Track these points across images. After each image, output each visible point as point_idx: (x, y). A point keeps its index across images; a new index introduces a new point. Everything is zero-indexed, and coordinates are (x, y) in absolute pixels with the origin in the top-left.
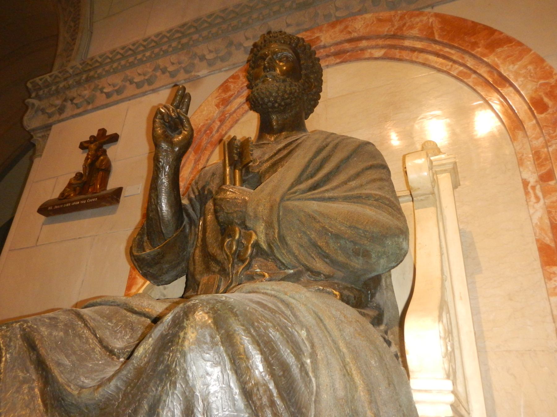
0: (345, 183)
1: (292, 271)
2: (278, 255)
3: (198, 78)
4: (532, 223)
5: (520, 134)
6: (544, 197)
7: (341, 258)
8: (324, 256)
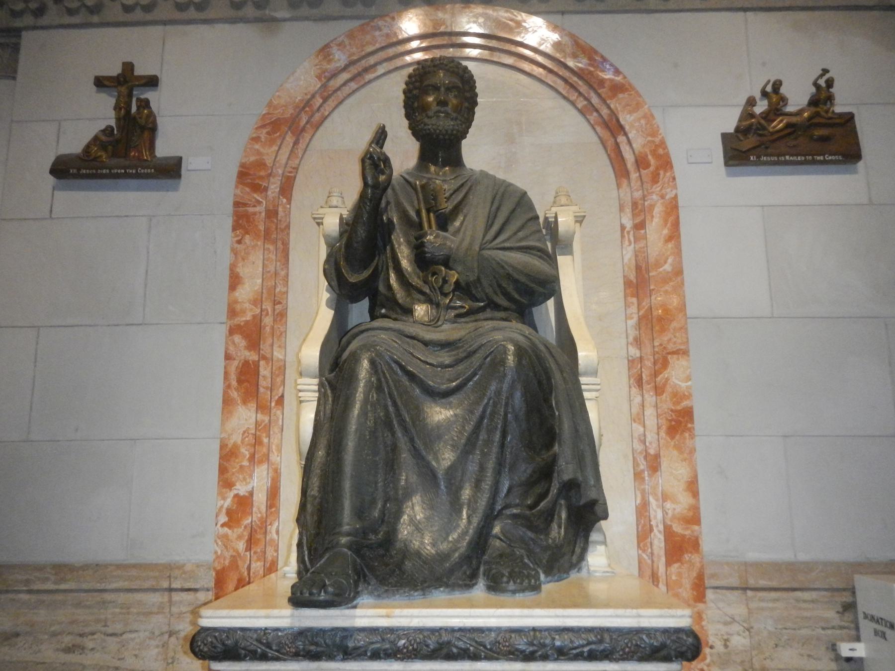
0: (515, 234)
1: (482, 304)
2: (474, 292)
3: (274, 20)
4: (623, 262)
5: (625, 182)
6: (635, 242)
7: (516, 296)
8: (506, 295)
